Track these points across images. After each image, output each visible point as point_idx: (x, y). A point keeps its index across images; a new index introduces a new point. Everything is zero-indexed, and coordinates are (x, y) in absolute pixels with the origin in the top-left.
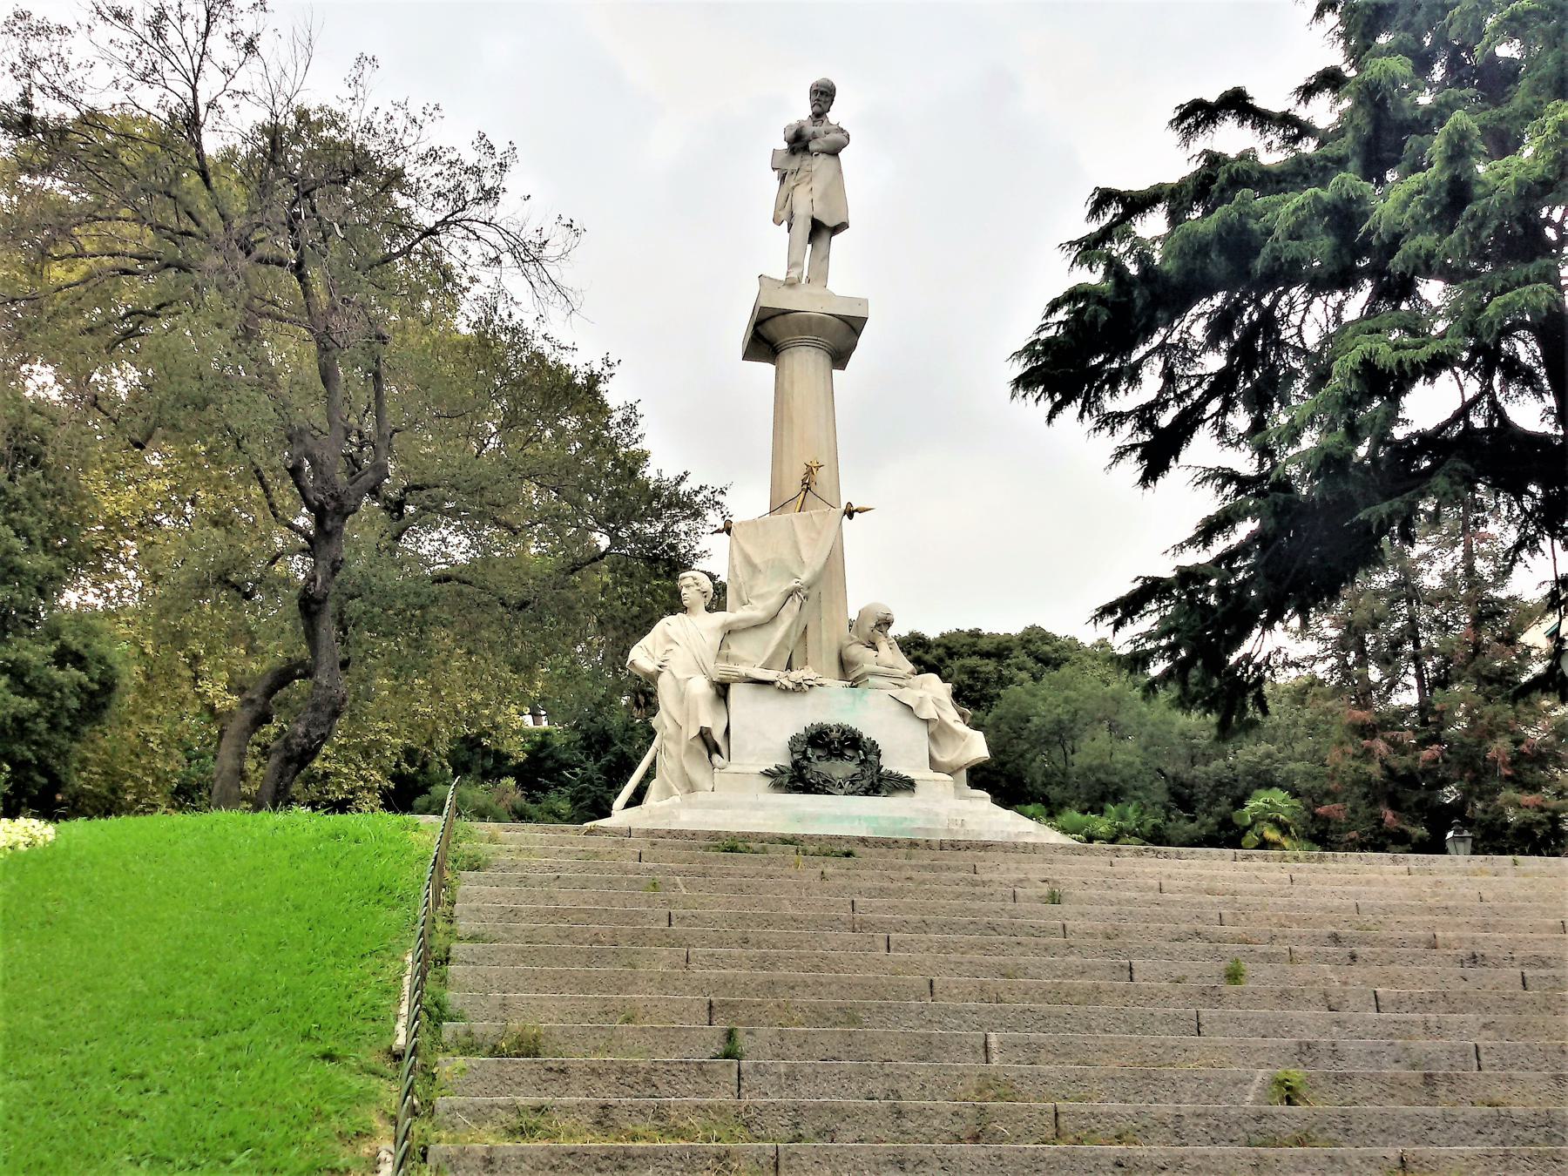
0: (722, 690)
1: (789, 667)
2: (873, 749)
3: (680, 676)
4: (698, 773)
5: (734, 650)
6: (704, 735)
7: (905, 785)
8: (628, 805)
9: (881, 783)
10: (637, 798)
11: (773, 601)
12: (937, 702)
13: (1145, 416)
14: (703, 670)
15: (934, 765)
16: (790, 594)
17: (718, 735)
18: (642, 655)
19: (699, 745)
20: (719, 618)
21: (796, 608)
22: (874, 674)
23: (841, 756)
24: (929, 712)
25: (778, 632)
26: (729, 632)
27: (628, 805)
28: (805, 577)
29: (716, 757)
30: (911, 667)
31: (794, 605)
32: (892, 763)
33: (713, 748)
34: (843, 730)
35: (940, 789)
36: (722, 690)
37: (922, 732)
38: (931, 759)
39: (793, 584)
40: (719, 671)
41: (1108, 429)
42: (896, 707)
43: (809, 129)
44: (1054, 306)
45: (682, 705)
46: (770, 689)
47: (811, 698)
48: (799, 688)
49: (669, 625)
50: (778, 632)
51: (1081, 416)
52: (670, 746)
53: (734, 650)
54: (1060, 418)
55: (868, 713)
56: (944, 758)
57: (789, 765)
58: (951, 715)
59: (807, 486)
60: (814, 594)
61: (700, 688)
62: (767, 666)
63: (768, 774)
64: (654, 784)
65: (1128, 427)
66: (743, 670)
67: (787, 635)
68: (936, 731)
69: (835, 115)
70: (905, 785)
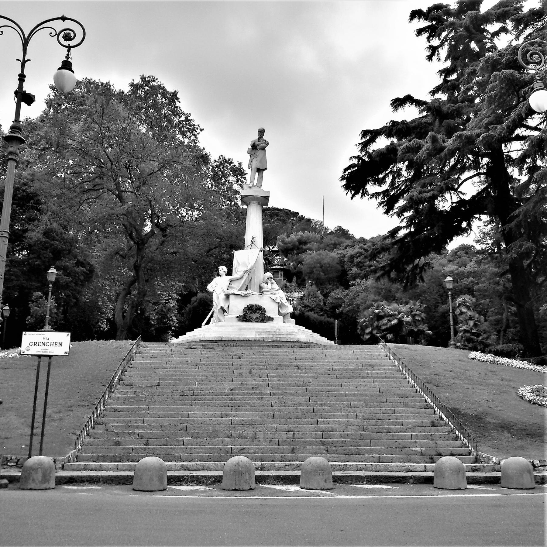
0: (228, 296)
1: (246, 289)
2: (264, 310)
3: (218, 293)
4: (221, 318)
5: (233, 285)
6: (222, 308)
7: (272, 319)
8: (206, 324)
9: (264, 319)
10: (208, 323)
11: (242, 273)
12: (281, 298)
13: (385, 193)
14: (224, 292)
15: (280, 314)
16: (246, 272)
17: (226, 308)
18: (210, 287)
19: (221, 310)
20: (230, 277)
21: (247, 275)
22: (266, 291)
23: (256, 312)
24: (279, 301)
25: (243, 281)
26: (231, 281)
27: (206, 324)
28: (249, 267)
29: (225, 313)
30: (278, 288)
31: (246, 275)
32: (267, 314)
33: (225, 311)
34: (256, 306)
35: (280, 319)
36: (228, 296)
37: (277, 307)
38: (279, 311)
39: (246, 269)
40: (227, 292)
41: (374, 198)
42: (270, 300)
43: (257, 143)
44: (346, 170)
45: (218, 301)
46: (239, 296)
47: (249, 298)
48: (246, 296)
49: (216, 280)
50: (243, 281)
51: (362, 197)
52: (215, 310)
53: (233, 285)
54: (354, 198)
55: (265, 302)
56: (283, 311)
57: (242, 314)
58: (285, 301)
59: (252, 242)
60: (253, 270)
61: (222, 296)
62: (240, 290)
63: (237, 317)
64: (212, 319)
65: (380, 197)
66: (232, 292)
67: (245, 282)
68: (281, 305)
69: (265, 137)
70: (272, 319)
